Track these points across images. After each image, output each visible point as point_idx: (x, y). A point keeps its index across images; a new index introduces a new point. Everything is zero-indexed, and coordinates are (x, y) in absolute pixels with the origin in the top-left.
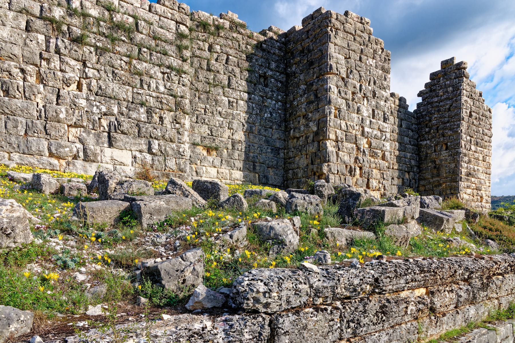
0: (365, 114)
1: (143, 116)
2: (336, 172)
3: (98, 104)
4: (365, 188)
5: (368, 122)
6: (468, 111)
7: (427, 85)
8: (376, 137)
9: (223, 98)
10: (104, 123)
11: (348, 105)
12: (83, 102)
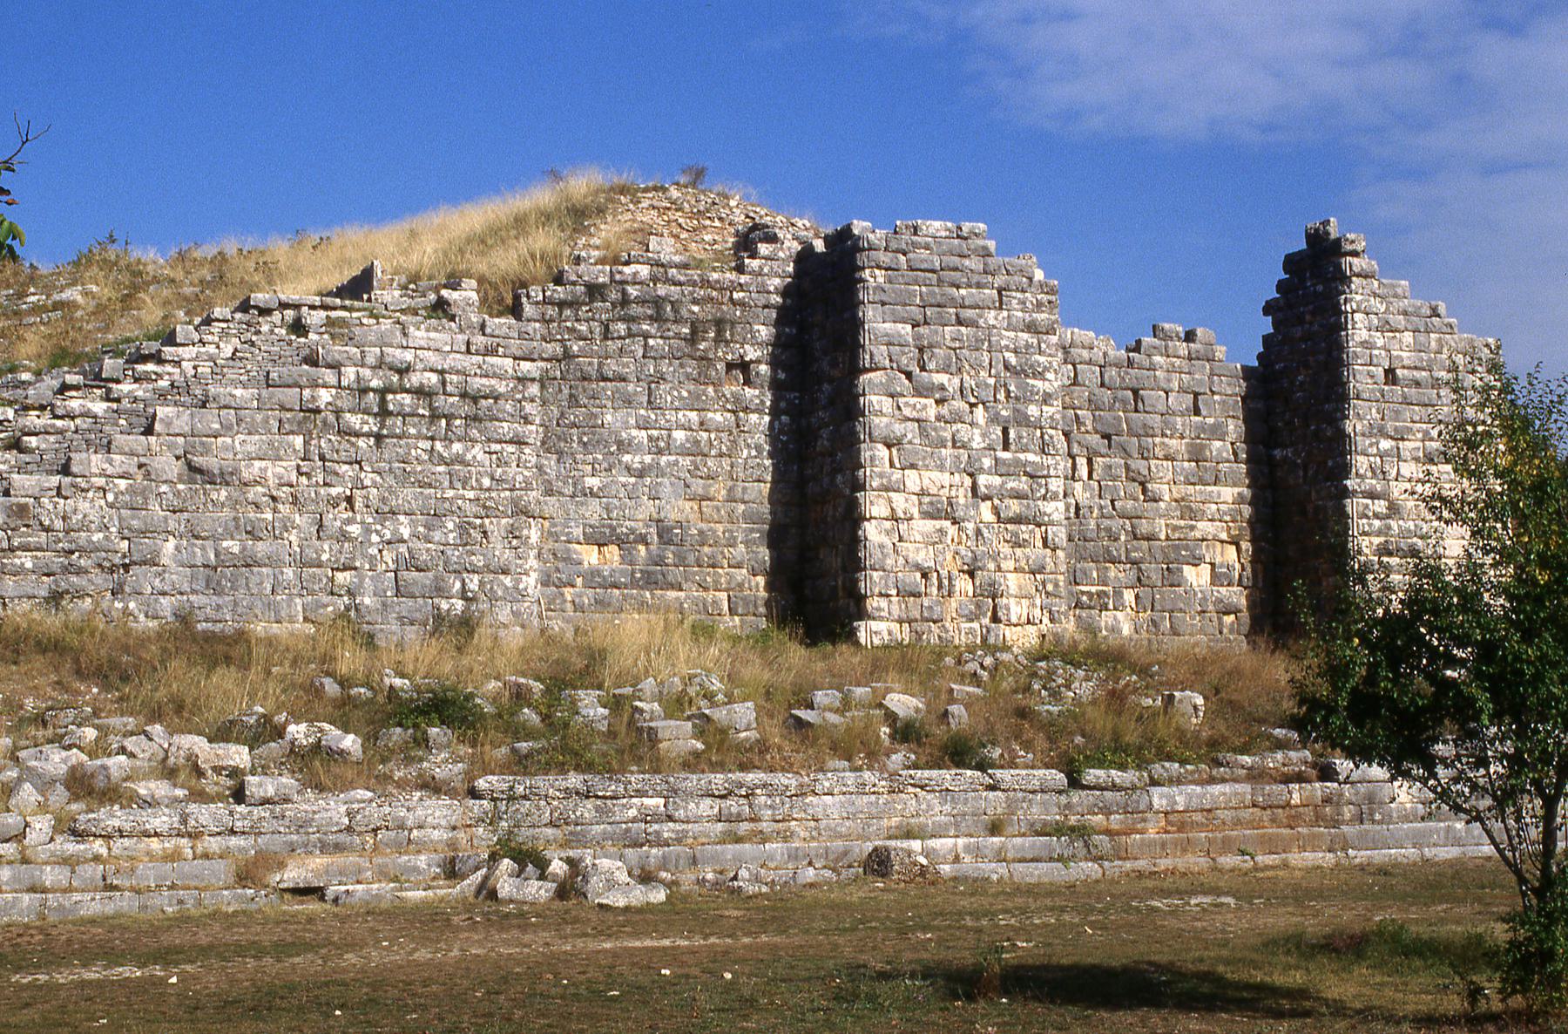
0: (978, 442)
1: (451, 536)
2: (894, 592)
3: (379, 527)
4: (986, 621)
5: (987, 462)
6: (1380, 372)
7: (1281, 286)
8: (1018, 496)
9: (634, 432)
10: (388, 557)
11: (923, 432)
12: (355, 529)
